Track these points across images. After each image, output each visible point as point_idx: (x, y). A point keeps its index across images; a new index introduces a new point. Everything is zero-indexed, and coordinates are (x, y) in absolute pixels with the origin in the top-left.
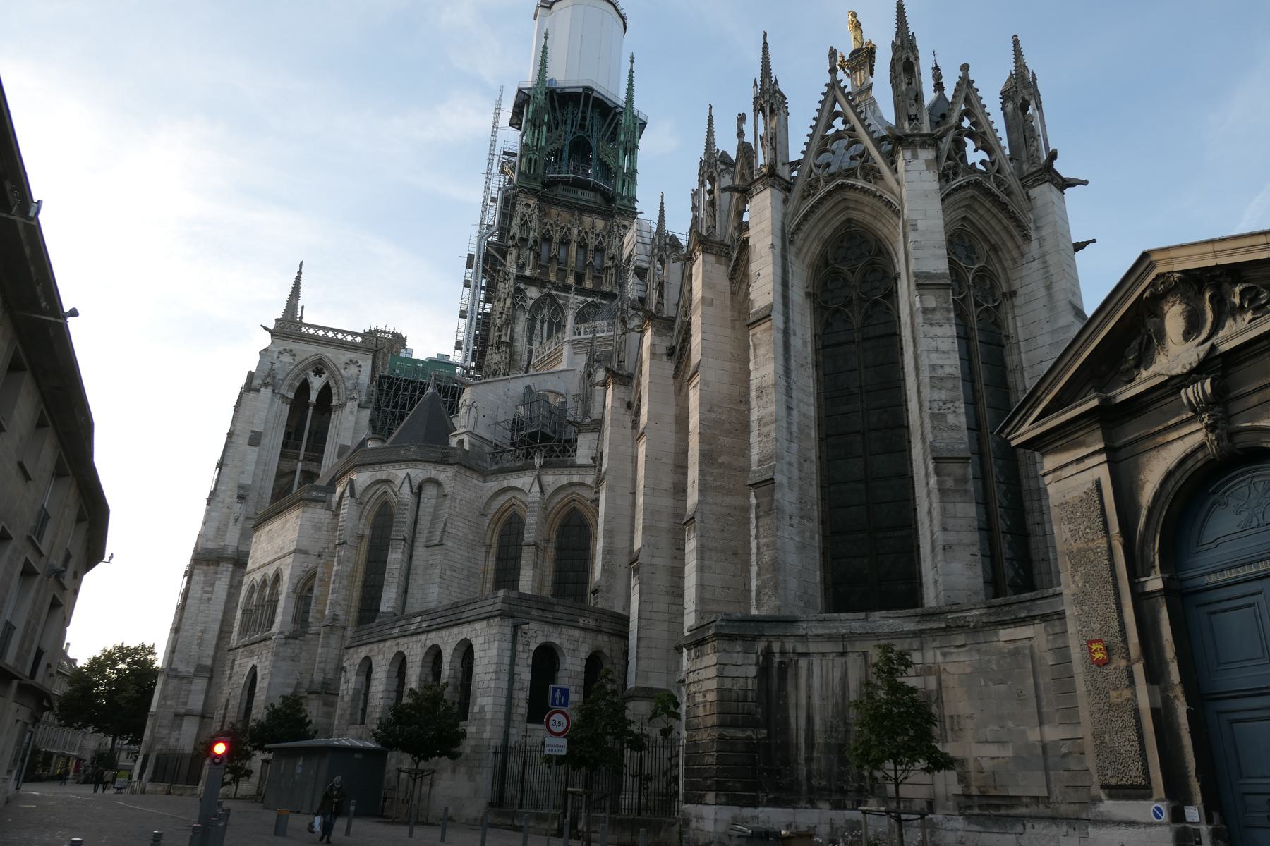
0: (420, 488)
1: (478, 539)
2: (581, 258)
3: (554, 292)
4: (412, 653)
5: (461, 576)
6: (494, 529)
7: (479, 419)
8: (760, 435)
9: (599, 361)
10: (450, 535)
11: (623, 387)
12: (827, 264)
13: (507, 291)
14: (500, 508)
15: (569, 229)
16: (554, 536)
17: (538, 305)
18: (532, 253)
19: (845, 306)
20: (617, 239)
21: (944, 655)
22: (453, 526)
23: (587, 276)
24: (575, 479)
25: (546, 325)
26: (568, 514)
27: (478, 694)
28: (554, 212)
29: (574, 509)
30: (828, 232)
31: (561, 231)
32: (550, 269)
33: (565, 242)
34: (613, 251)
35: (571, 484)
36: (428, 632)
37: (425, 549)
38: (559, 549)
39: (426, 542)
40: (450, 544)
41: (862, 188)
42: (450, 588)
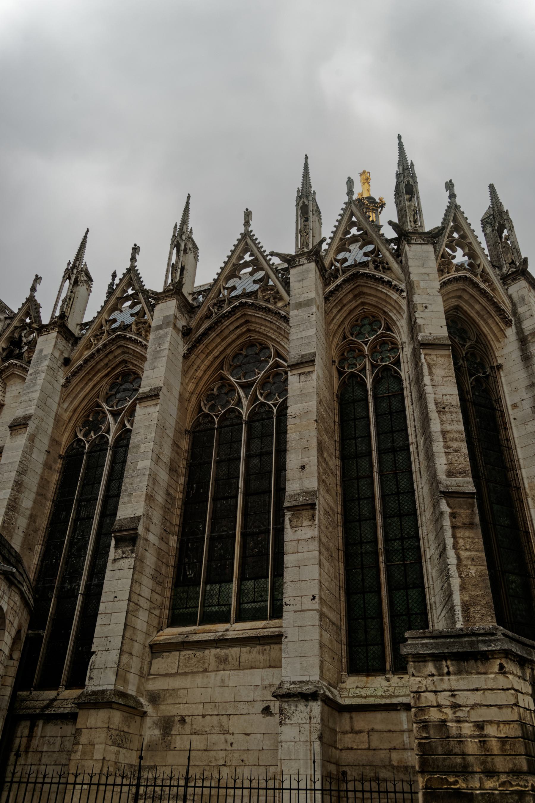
8: (446, 447)
11: (65, 342)
41: (483, 289)
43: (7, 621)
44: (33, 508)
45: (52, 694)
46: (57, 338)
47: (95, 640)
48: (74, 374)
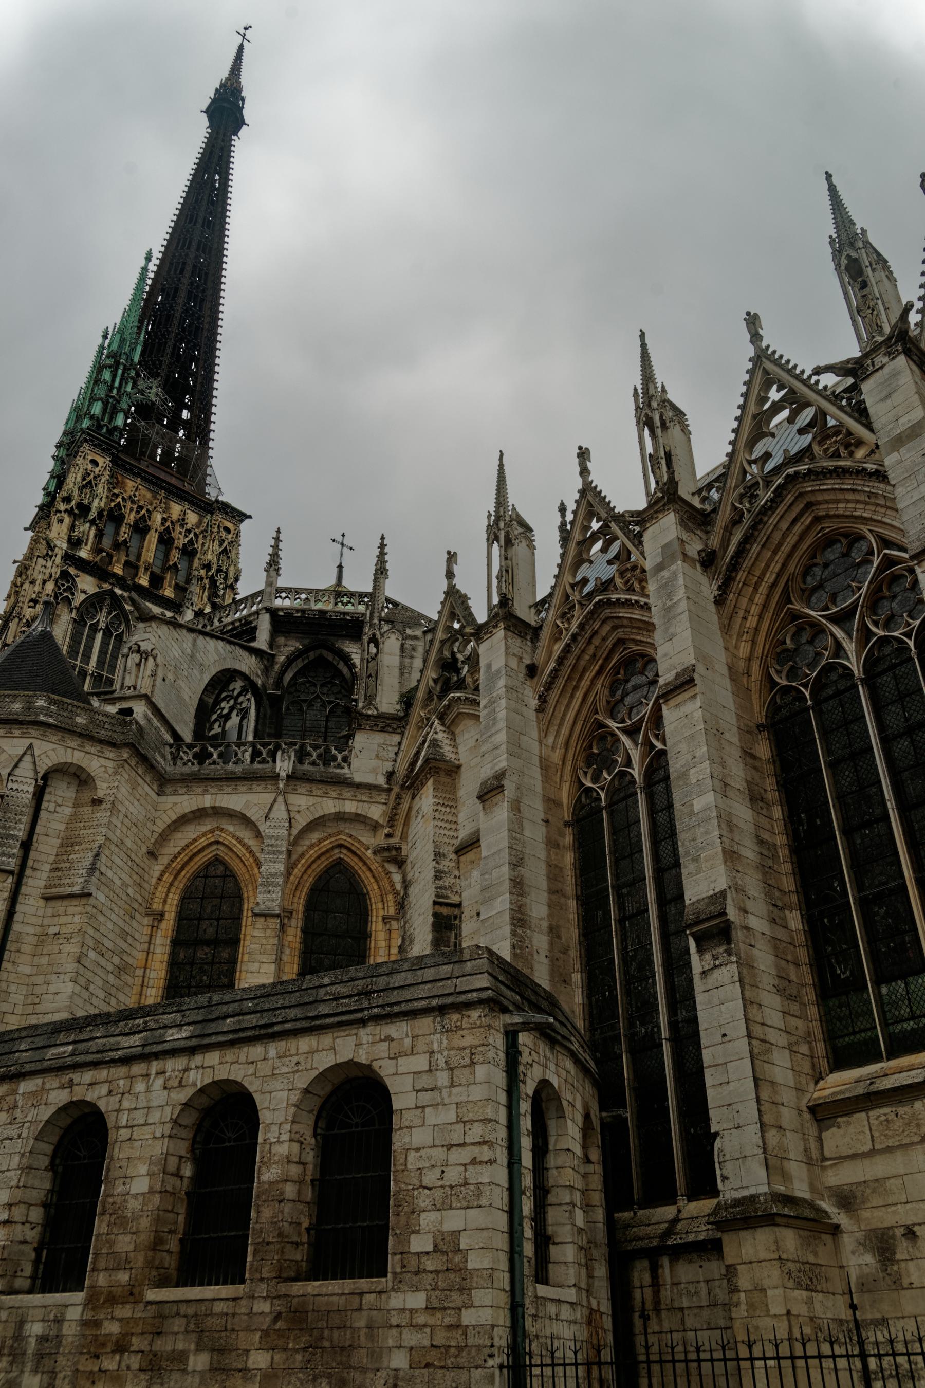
0: (45, 777)
1: (140, 900)
2: (161, 556)
3: (118, 591)
4: (126, 1104)
5: (110, 968)
6: (171, 885)
9: (388, 621)
10: (103, 879)
11: (519, 640)
13: (47, 571)
14: (191, 843)
15: (148, 511)
16: (299, 906)
17: (94, 603)
18: (94, 528)
20: (216, 542)
22: (109, 865)
23: (166, 582)
24: (350, 807)
25: (99, 636)
27: (423, 1199)
28: (130, 484)
29: (339, 862)
31: (138, 512)
32: (114, 559)
33: (141, 529)
34: (209, 557)
35: (340, 817)
36: (191, 1051)
37: (42, 903)
38: (308, 931)
39: (46, 887)
40: (101, 897)
42: (92, 987)
43: (565, 1103)
44: (550, 915)
45: (668, 1212)
46: (505, 638)
47: (712, 1113)
48: (549, 687)
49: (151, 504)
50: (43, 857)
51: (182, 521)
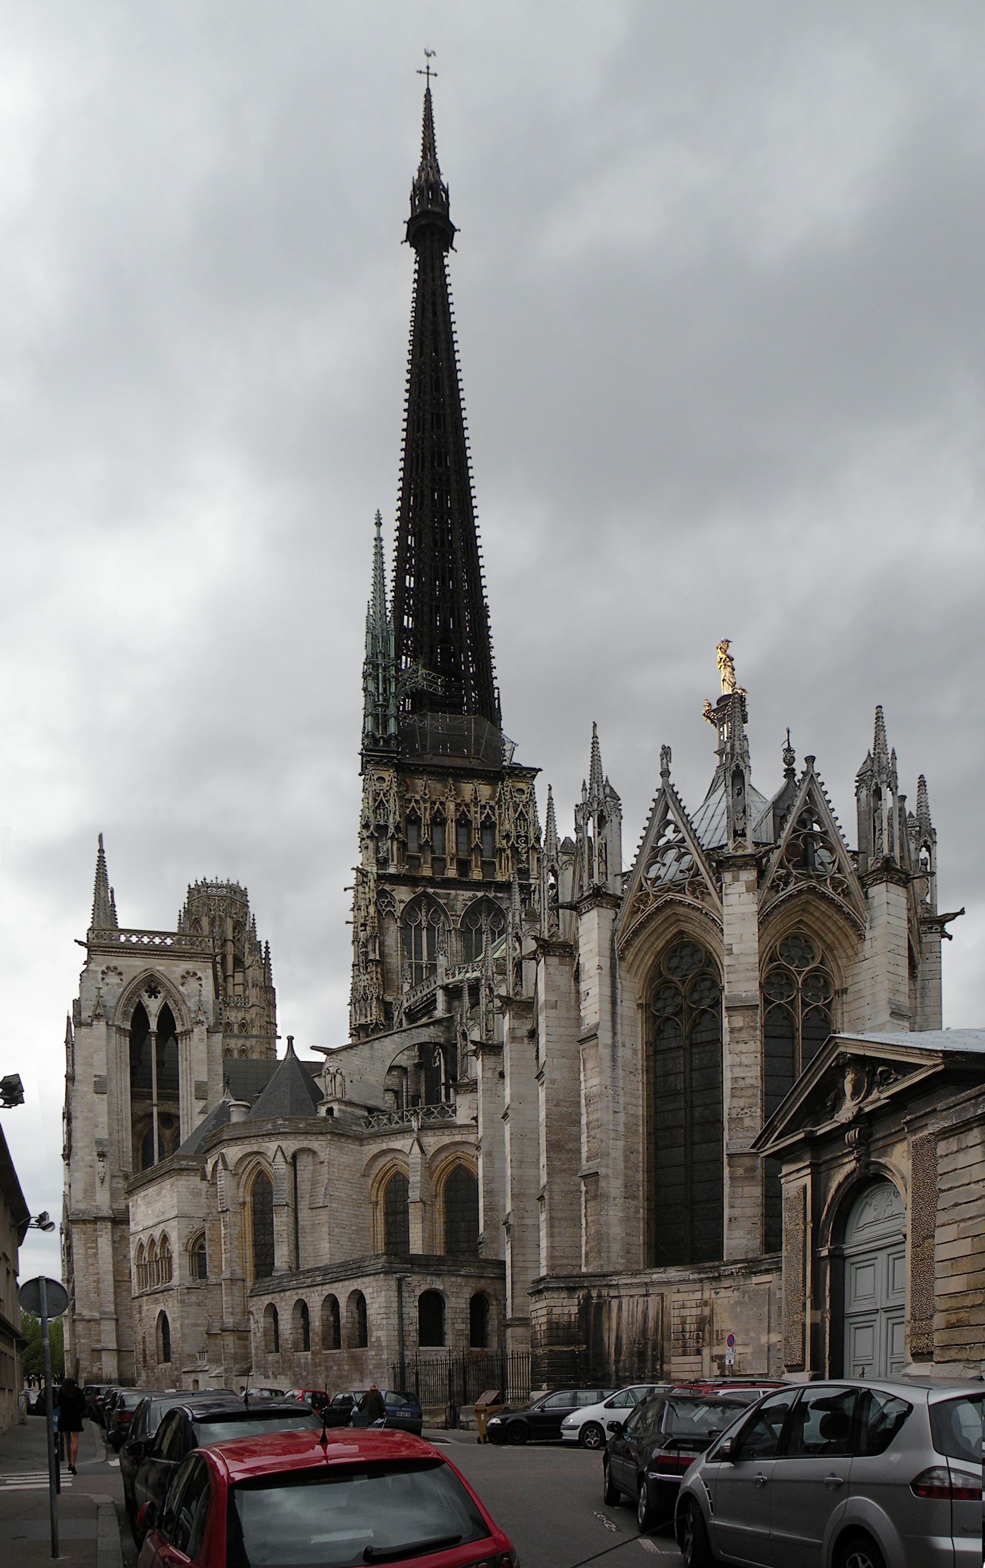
0: (294, 1157)
2: (463, 839)
7: (347, 1086)
12: (660, 974)
15: (442, 803)
19: (675, 1014)
21: (717, 1293)
26: (455, 1170)
30: (660, 944)
49: (443, 795)
50: (305, 1191)
51: (476, 801)
